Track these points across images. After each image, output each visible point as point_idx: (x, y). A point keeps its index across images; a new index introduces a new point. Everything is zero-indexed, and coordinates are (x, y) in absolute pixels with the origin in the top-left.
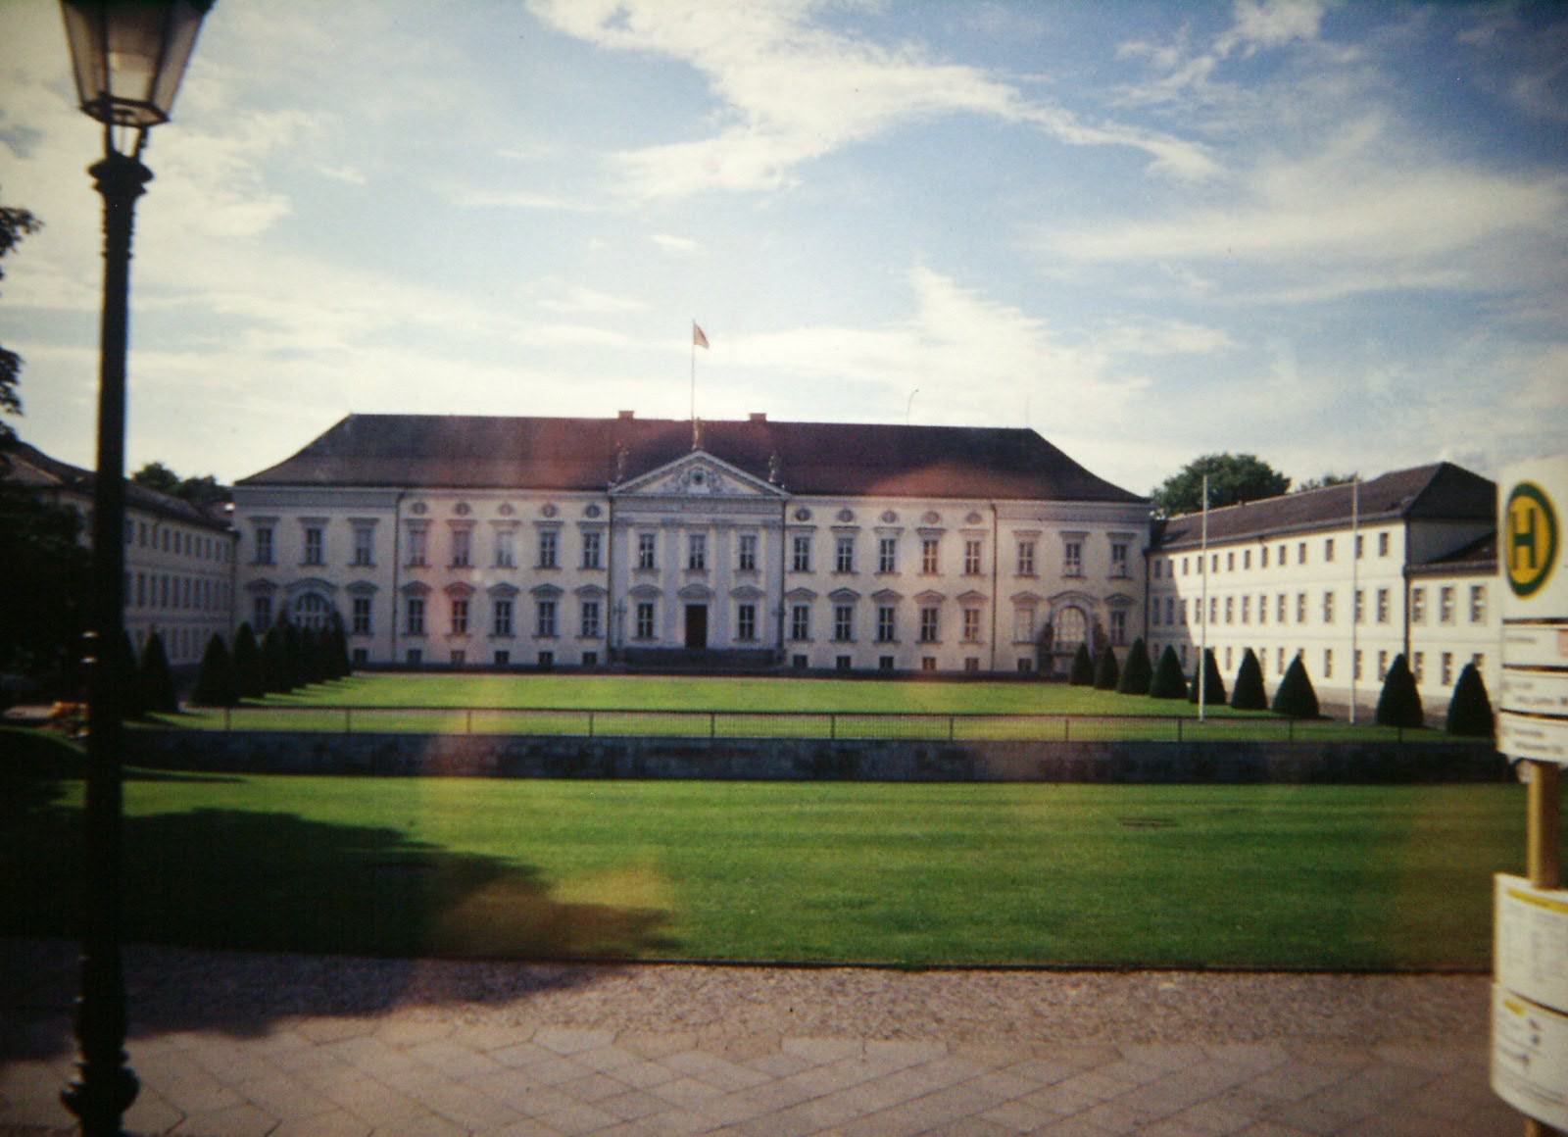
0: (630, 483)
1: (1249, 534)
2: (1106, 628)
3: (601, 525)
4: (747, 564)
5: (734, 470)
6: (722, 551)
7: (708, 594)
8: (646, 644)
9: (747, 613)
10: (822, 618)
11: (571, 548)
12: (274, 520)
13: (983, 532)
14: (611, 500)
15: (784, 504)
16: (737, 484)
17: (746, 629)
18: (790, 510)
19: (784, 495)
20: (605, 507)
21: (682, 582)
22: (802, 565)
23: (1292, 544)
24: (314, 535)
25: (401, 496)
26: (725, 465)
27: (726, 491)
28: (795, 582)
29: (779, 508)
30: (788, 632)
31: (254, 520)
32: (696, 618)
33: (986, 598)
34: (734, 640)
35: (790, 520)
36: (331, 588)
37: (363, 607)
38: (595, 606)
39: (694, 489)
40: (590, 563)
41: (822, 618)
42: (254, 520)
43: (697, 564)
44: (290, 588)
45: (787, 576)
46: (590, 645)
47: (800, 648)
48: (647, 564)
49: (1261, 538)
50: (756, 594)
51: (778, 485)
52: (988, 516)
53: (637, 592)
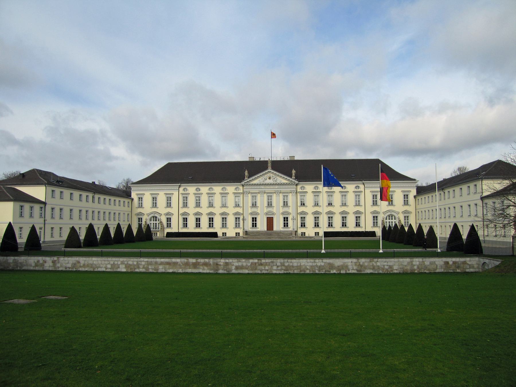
0: (248, 180)
1: (440, 188)
2: (403, 222)
3: (239, 193)
4: (285, 204)
5: (280, 175)
6: (277, 200)
7: (273, 214)
8: (254, 230)
9: (286, 219)
10: (310, 221)
11: (231, 200)
12: (144, 194)
13: (361, 192)
14: (243, 186)
15: (297, 185)
16: (281, 179)
17: (286, 225)
18: (299, 187)
19: (297, 182)
20: (241, 188)
21: (266, 210)
22: (303, 204)
23: (451, 190)
24: (154, 199)
25: (180, 186)
26: (278, 173)
27: (278, 182)
28: (301, 209)
29: (295, 187)
30: (299, 225)
31: (137, 194)
32: (270, 221)
33: (362, 213)
34: (282, 228)
35: (299, 190)
36: (161, 215)
37: (169, 220)
38: (239, 218)
39: (268, 181)
40: (237, 205)
41: (310, 221)
42: (137, 194)
43: (270, 205)
44: (148, 215)
45: (298, 206)
46: (238, 230)
47: (303, 230)
48: (254, 205)
49: (443, 189)
50: (289, 214)
51: (294, 179)
52: (362, 186)
53: (251, 214)
